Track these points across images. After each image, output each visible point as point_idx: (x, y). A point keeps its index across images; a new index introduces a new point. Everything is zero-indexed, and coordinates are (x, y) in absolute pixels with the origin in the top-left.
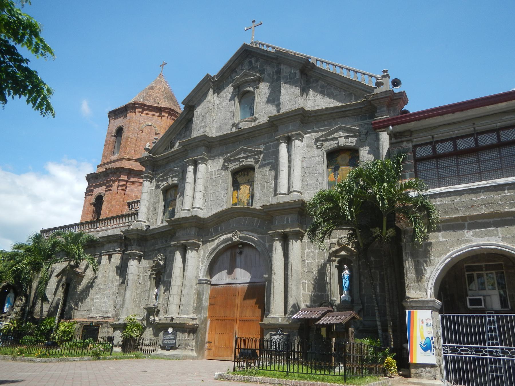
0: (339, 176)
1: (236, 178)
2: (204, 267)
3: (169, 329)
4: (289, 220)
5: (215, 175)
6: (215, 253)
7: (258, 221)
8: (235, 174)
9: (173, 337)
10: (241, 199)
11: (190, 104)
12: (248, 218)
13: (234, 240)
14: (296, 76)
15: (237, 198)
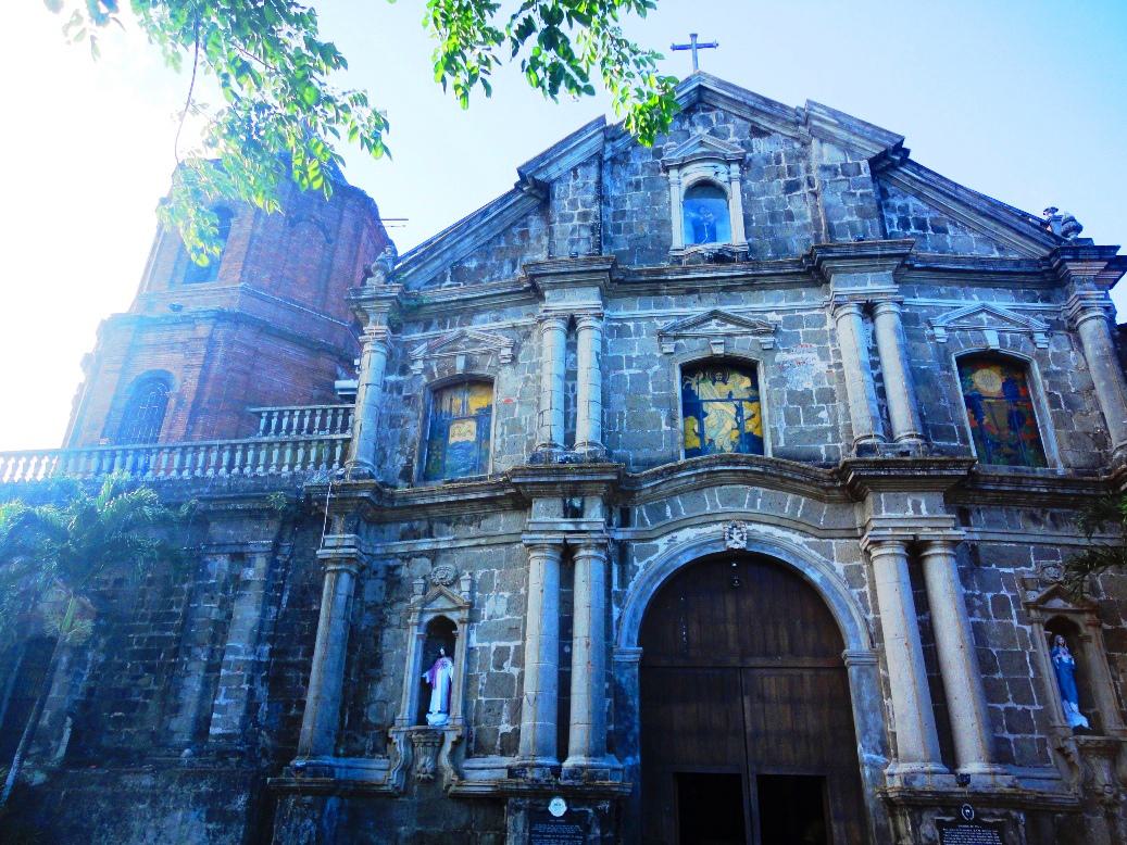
0: (986, 421)
1: (689, 385)
2: (628, 613)
3: (554, 801)
4: (923, 507)
5: (629, 367)
6: (662, 579)
7: (796, 504)
8: (689, 370)
9: (571, 829)
10: (711, 441)
11: (541, 177)
12: (761, 490)
13: (730, 544)
14: (859, 173)
15: (697, 434)
